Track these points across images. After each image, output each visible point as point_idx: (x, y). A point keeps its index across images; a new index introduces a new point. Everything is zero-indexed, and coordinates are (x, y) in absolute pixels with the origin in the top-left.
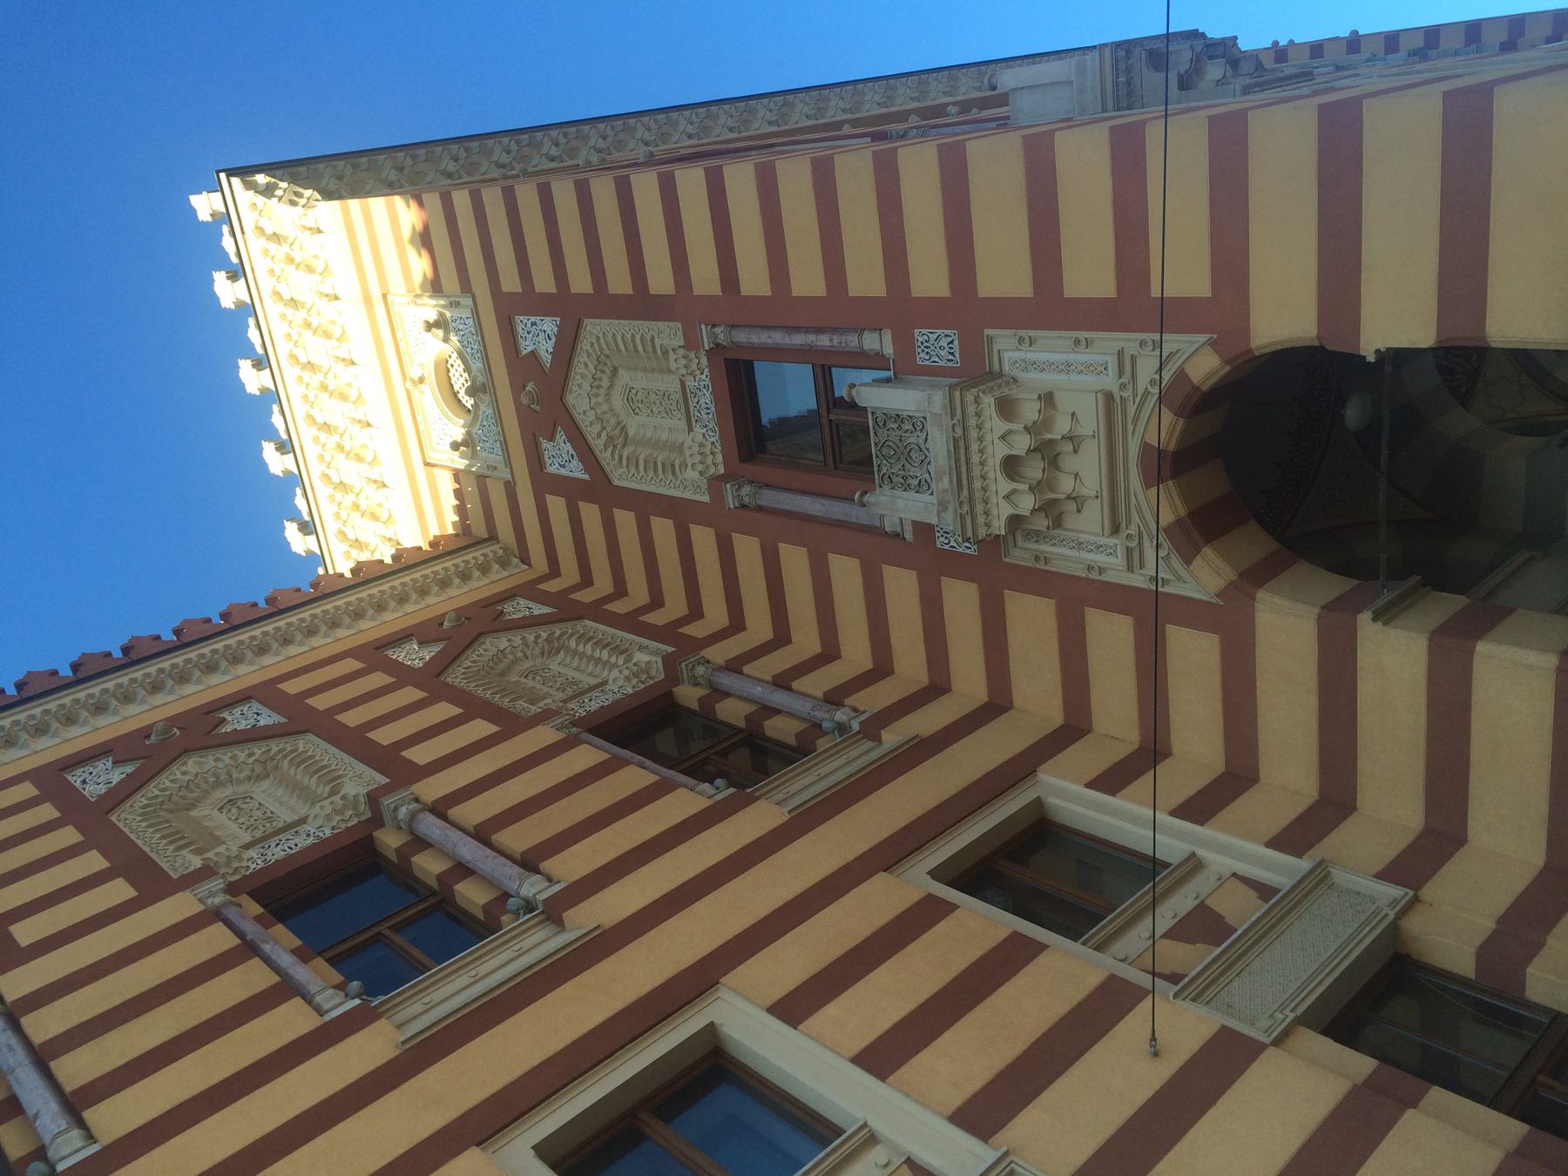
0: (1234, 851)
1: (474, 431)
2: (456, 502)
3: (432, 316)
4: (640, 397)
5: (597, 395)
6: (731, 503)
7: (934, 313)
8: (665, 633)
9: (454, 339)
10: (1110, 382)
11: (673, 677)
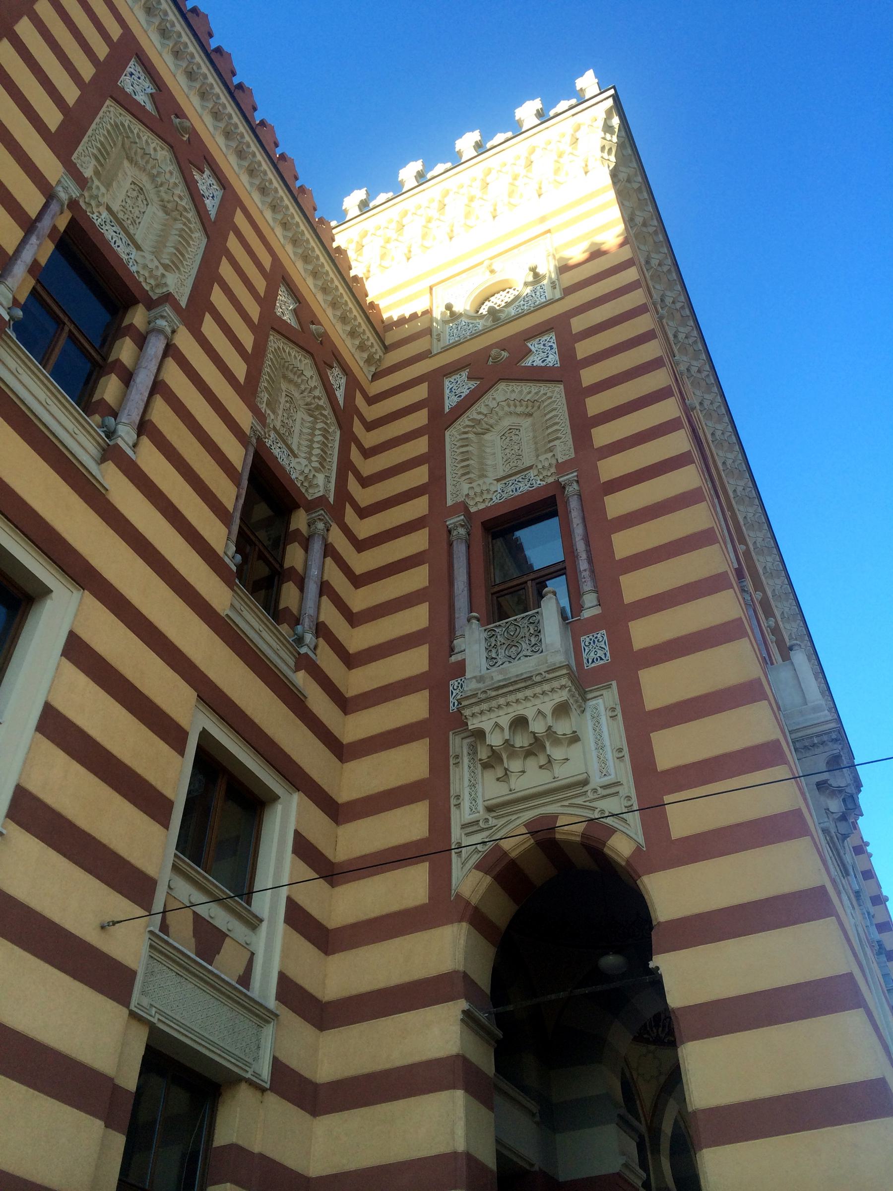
0: (271, 950)
1: (463, 319)
2: (407, 316)
3: (541, 271)
4: (514, 438)
5: (509, 406)
7: (620, 641)
9: (528, 290)
10: (596, 780)
11: (311, 506)
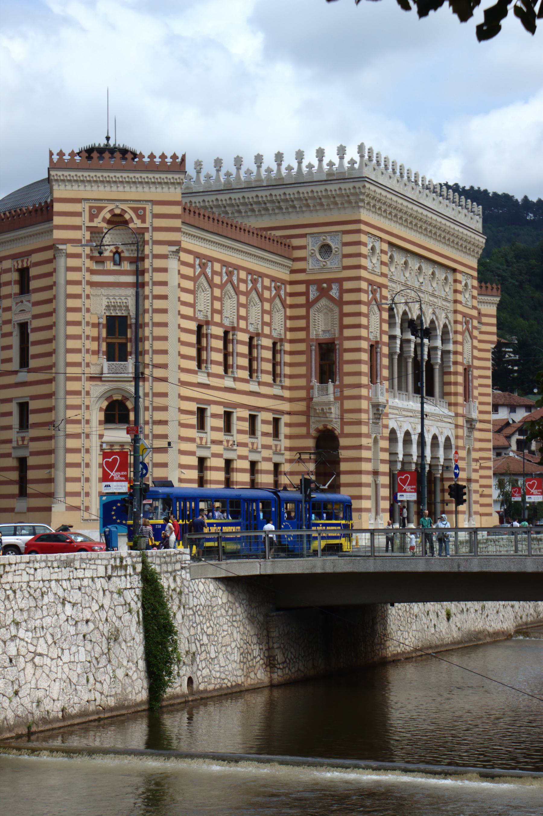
6: (311, 343)
8: (287, 329)
